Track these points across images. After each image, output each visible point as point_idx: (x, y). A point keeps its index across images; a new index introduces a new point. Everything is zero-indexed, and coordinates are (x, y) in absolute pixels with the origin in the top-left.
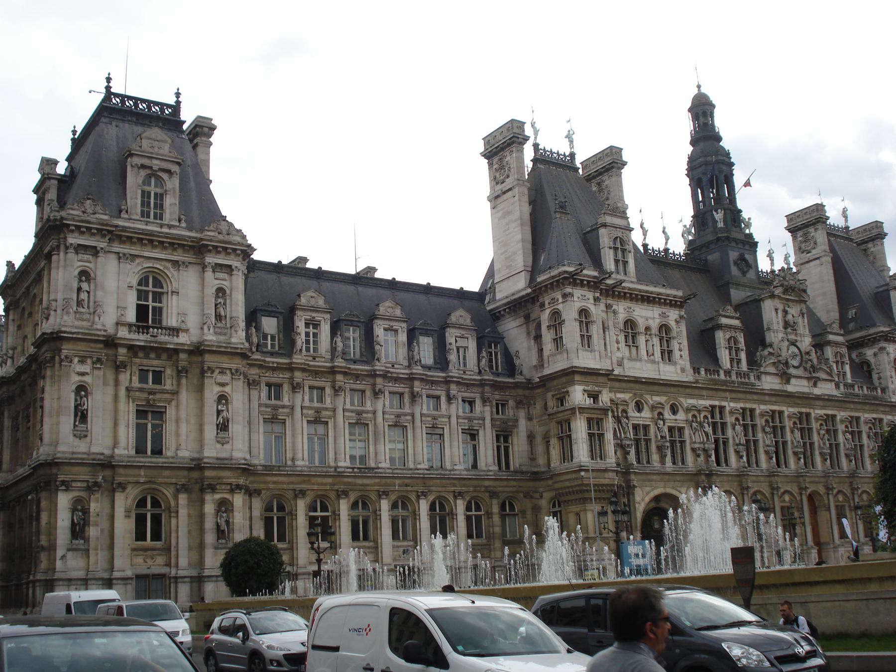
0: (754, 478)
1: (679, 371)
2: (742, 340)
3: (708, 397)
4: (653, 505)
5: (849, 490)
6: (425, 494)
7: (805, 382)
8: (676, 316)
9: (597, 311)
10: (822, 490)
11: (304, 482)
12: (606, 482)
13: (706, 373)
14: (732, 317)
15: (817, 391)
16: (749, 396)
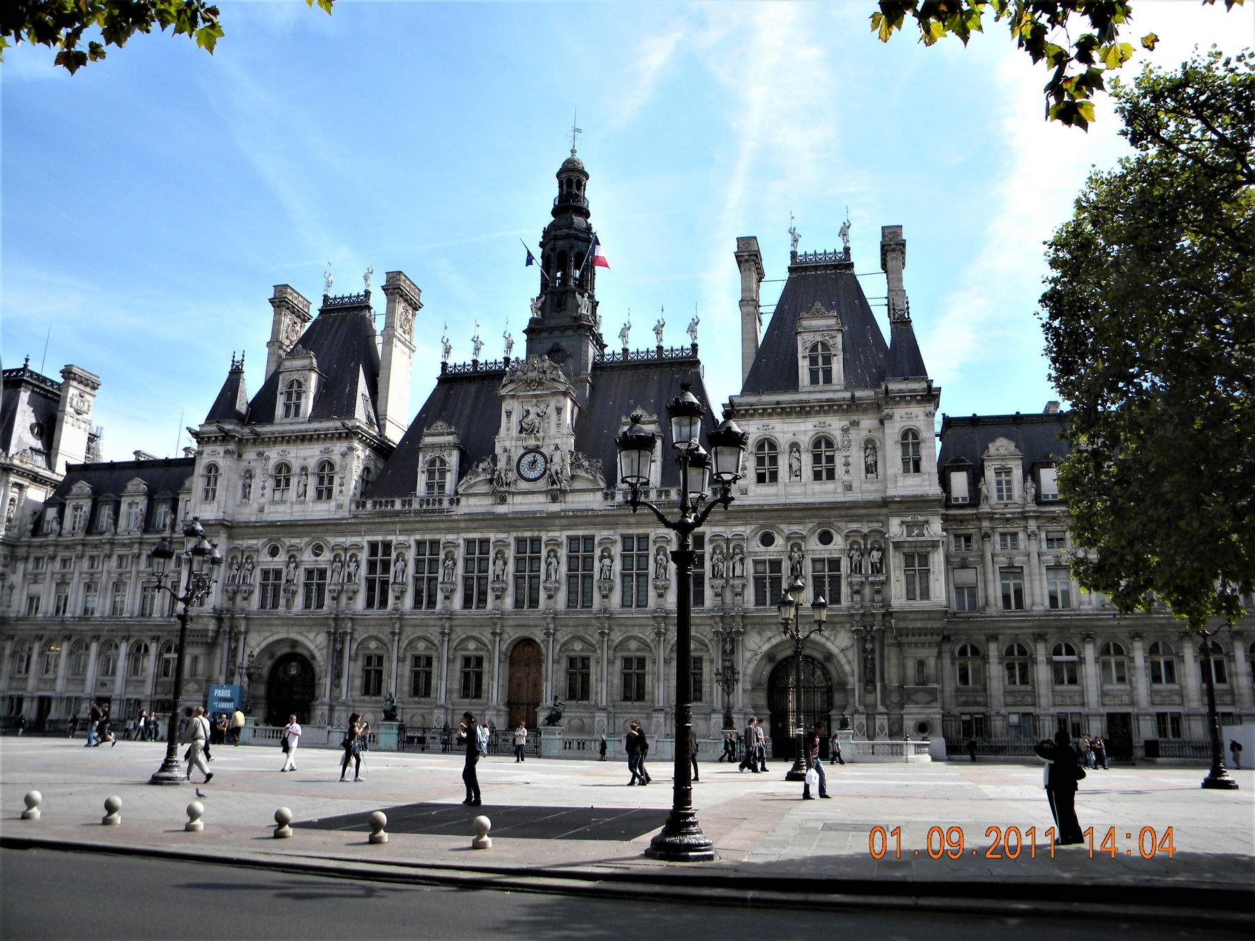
0: (418, 622)
1: (333, 509)
2: (453, 459)
3: (367, 533)
4: (286, 650)
5: (597, 636)
6: (126, 638)
7: (541, 498)
8: (345, 449)
9: (223, 463)
10: (538, 636)
11: (43, 629)
12: (199, 627)
13: (374, 506)
14: (442, 434)
15: (555, 507)
16: (431, 525)
